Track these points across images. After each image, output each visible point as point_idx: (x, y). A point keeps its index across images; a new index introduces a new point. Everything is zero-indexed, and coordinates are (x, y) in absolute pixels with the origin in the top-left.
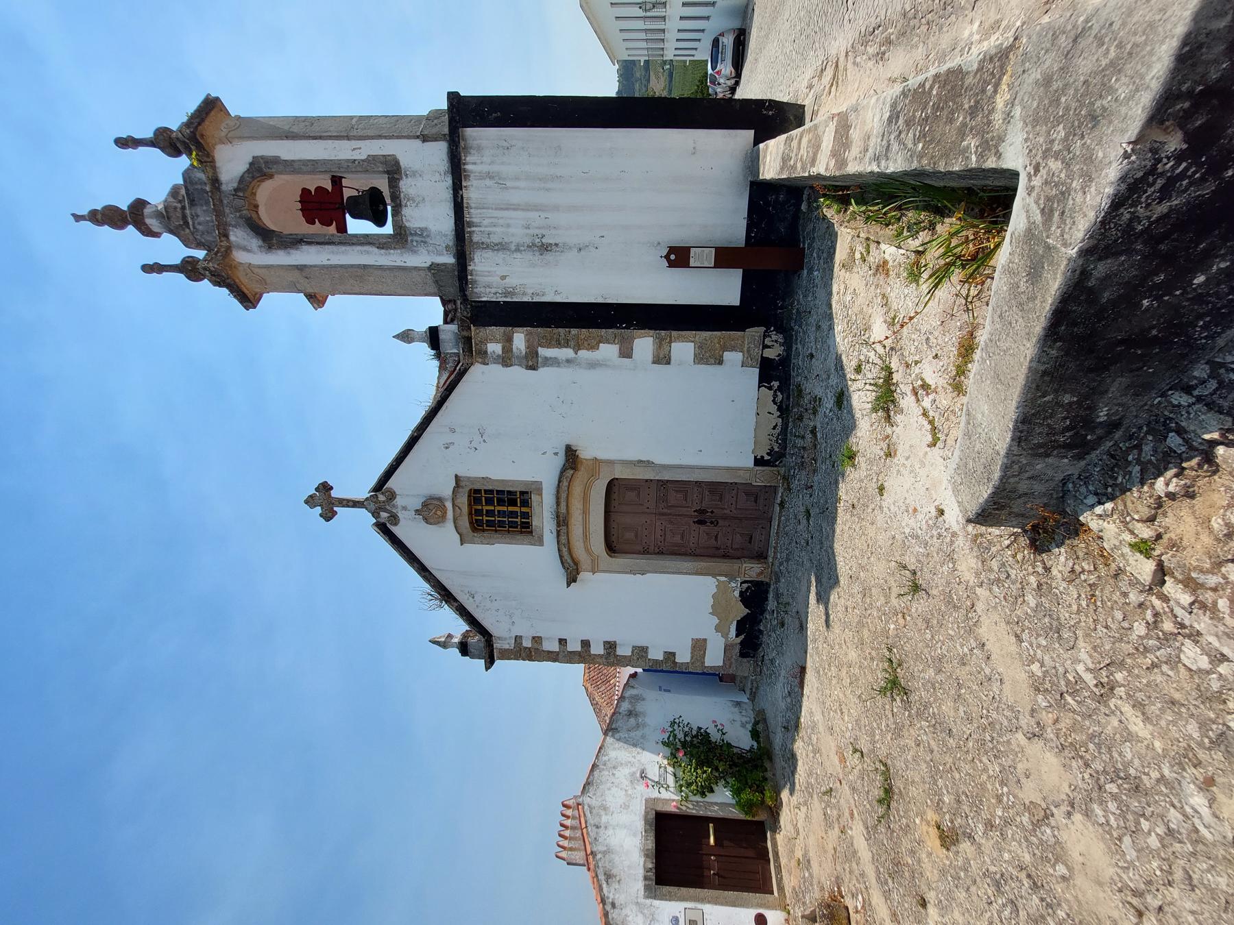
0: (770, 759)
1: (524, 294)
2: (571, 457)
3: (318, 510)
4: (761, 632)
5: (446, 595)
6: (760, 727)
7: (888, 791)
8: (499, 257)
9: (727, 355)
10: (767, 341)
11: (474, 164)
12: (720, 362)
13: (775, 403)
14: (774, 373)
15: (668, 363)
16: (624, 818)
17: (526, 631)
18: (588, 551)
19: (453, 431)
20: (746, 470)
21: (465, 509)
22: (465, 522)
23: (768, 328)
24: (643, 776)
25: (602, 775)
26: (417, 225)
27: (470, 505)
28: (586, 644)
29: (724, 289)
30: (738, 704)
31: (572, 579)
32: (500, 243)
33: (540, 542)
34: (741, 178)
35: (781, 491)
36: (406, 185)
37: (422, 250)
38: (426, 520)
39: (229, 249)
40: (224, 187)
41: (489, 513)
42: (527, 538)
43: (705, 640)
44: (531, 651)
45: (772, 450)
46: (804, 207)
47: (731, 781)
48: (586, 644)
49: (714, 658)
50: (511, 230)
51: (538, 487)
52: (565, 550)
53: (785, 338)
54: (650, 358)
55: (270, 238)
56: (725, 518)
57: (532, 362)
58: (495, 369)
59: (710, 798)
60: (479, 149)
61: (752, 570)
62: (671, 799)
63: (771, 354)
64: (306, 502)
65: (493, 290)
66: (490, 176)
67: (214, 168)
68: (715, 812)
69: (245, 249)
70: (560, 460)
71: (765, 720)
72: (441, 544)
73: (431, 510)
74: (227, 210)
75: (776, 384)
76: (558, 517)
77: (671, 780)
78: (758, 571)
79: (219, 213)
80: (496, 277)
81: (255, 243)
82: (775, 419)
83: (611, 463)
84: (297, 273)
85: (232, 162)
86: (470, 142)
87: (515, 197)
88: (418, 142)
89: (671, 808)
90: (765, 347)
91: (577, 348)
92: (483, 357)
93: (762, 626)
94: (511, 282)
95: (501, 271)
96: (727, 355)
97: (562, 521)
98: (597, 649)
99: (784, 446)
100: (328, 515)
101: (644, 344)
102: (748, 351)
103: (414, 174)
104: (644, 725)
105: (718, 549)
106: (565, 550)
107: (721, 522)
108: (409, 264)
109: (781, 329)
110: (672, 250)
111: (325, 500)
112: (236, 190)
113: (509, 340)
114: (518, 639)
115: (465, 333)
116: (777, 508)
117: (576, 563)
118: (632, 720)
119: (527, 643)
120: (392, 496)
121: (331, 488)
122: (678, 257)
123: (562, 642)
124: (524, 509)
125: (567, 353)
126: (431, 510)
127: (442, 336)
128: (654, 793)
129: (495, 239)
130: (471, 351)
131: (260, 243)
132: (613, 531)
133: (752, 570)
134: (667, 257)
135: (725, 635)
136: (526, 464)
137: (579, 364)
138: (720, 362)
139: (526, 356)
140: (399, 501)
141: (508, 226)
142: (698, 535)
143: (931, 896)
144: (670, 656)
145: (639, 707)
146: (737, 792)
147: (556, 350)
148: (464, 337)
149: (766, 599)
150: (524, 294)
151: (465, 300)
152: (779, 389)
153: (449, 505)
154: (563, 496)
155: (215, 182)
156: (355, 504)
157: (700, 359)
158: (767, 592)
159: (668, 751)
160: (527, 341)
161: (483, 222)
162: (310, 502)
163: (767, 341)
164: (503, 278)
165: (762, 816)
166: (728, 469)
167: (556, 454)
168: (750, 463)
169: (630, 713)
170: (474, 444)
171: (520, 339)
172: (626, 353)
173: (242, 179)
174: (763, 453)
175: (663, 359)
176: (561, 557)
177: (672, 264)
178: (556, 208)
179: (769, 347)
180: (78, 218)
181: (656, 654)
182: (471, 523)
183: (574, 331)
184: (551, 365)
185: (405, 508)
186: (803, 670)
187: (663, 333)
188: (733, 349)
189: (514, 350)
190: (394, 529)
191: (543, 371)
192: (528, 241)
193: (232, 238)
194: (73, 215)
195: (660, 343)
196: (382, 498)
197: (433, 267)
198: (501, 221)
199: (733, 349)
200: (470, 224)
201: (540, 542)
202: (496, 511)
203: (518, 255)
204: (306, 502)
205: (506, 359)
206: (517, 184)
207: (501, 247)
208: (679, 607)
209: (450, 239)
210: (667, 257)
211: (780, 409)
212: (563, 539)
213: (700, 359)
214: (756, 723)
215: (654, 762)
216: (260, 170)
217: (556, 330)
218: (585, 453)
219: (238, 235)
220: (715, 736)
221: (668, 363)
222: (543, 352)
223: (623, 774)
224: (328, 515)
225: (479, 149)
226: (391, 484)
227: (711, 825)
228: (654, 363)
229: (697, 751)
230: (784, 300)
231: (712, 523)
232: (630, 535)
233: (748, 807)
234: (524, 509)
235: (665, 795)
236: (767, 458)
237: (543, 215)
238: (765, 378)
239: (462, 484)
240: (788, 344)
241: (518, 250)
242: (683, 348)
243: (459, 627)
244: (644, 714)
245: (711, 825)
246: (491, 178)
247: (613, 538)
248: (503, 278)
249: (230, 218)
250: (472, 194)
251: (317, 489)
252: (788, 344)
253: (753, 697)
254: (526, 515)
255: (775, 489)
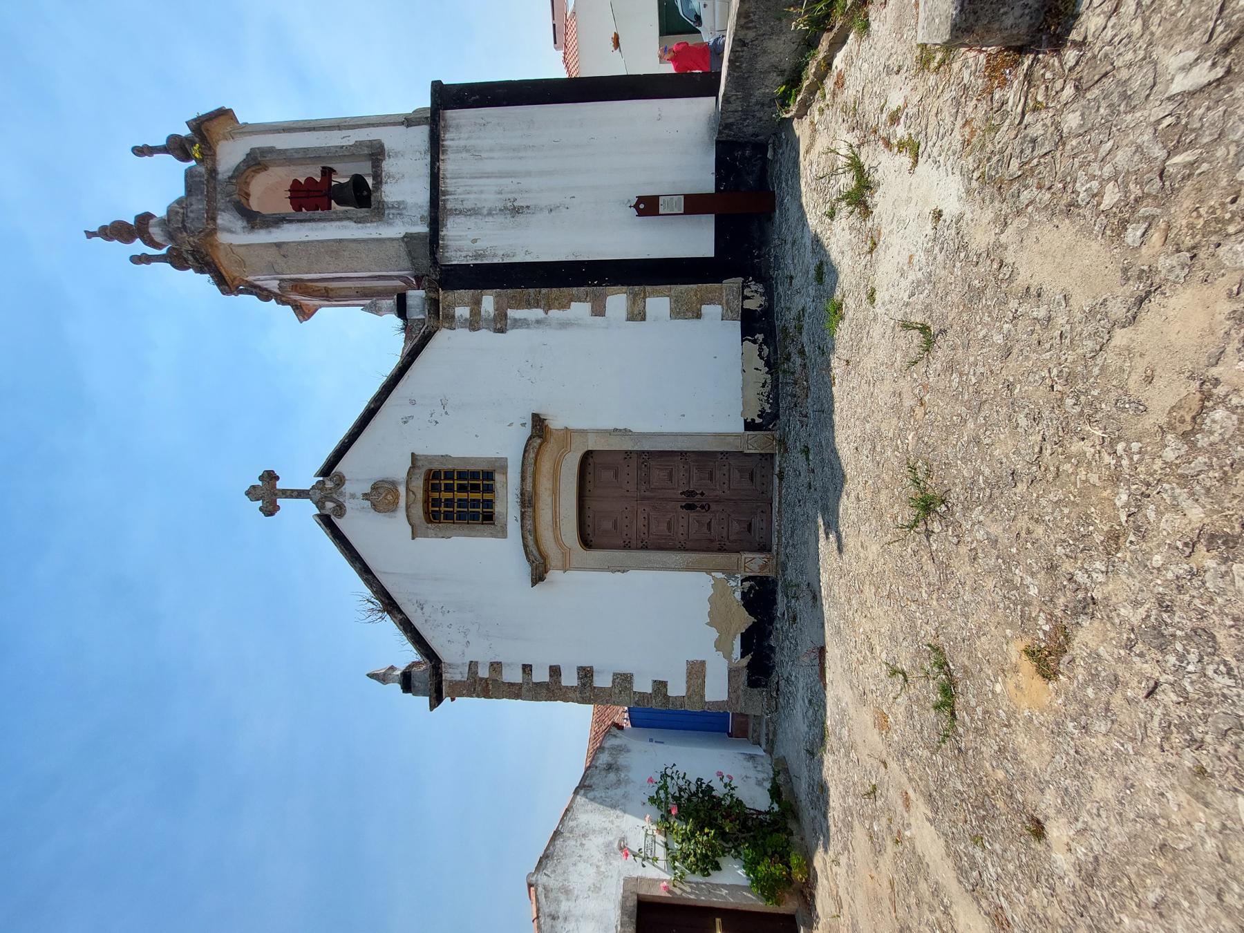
0: (796, 817)
1: (495, 255)
2: (539, 424)
3: (260, 503)
4: (772, 649)
5: (390, 605)
6: (781, 779)
7: (948, 691)
8: (471, 222)
9: (706, 309)
10: (747, 292)
11: (451, 140)
12: (698, 316)
13: (762, 358)
14: (754, 325)
15: (644, 319)
16: (591, 905)
17: (483, 655)
18: (557, 540)
19: (413, 403)
20: (737, 435)
21: (420, 495)
22: (418, 510)
23: (746, 279)
24: (624, 849)
25: (569, 845)
26: (394, 199)
27: (426, 491)
28: (555, 671)
29: (696, 239)
30: (752, 757)
31: (538, 577)
32: (473, 209)
33: (503, 533)
34: (706, 138)
35: (777, 459)
36: (388, 166)
37: (398, 221)
38: (375, 507)
39: (213, 232)
40: (220, 177)
41: (449, 503)
42: (487, 528)
43: (703, 663)
44: (487, 685)
45: (763, 411)
46: (770, 155)
47: (745, 848)
48: (555, 671)
49: (717, 690)
50: (483, 196)
51: (502, 465)
52: (530, 538)
53: (765, 288)
54: (624, 315)
55: (254, 220)
56: (718, 501)
57: (500, 324)
58: (462, 334)
59: (716, 878)
60: (458, 127)
61: (754, 563)
62: (659, 877)
63: (752, 305)
64: (248, 493)
65: (464, 254)
66: (466, 149)
67: (214, 161)
68: (723, 899)
69: (230, 231)
70: (527, 431)
71: (786, 771)
72: (388, 537)
73: (381, 496)
74: (219, 197)
75: (760, 337)
76: (522, 494)
77: (660, 852)
78: (761, 562)
79: (211, 199)
80: (466, 241)
81: (240, 224)
82: (763, 375)
83: (583, 432)
84: (274, 250)
85: (230, 155)
86: (450, 122)
87: (488, 166)
88: (403, 128)
89: (660, 892)
90: (745, 298)
91: (548, 307)
92: (450, 321)
93: (771, 629)
94: (480, 245)
95: (472, 235)
96: (706, 309)
97: (528, 502)
98: (570, 679)
99: (776, 404)
100: (270, 510)
101: (617, 301)
102: (727, 303)
103: (396, 154)
104: (627, 782)
105: (711, 541)
106: (530, 538)
107: (714, 507)
108: (384, 236)
109: (758, 279)
110: (641, 199)
111: (268, 493)
112: (230, 178)
113: (478, 302)
114: (473, 665)
115: (432, 295)
116: (776, 481)
117: (544, 558)
118: (612, 776)
119: (484, 673)
120: (341, 481)
121: (277, 478)
122: (648, 206)
123: (527, 669)
124: (487, 496)
125: (538, 313)
126: (381, 496)
127: (410, 302)
128: (635, 869)
129: (468, 205)
130: (438, 315)
131: (245, 224)
132: (589, 521)
133: (754, 563)
134: (636, 206)
135: (728, 656)
136: (492, 440)
137: (549, 325)
138: (698, 316)
139: (495, 319)
140: (348, 488)
141: (482, 192)
142: (687, 523)
143: (1047, 804)
144: (660, 686)
145: (622, 760)
146: (751, 866)
147: (526, 311)
148: (431, 299)
149: (774, 602)
150: (495, 255)
151: (435, 262)
152: (765, 342)
153: (402, 490)
154: (530, 470)
155: (213, 172)
156: (301, 494)
157: (679, 312)
158: (774, 592)
159: (656, 813)
160: (496, 303)
161: (457, 190)
162: (252, 493)
163: (747, 292)
164: (474, 241)
165: (789, 906)
166: (717, 435)
167: (523, 425)
168: (740, 428)
169: (609, 767)
170: (434, 418)
171: (488, 302)
172: (599, 311)
173: (237, 168)
174: (753, 415)
175: (636, 315)
176: (525, 546)
177: (641, 213)
178: (528, 174)
179: (749, 298)
180: (90, 235)
181: (643, 685)
182: (426, 513)
183: (544, 291)
184: (520, 327)
185: (353, 496)
186: (822, 651)
187: (637, 288)
188: (711, 302)
189: (483, 313)
190: (340, 523)
191: (512, 335)
192: (500, 205)
193: (219, 221)
194: (86, 232)
195: (634, 299)
196: (329, 484)
197: (409, 239)
198: (475, 189)
199: (711, 302)
200: (445, 193)
201: (503, 533)
202: (454, 497)
203: (491, 219)
204: (248, 493)
205: (474, 324)
206: (491, 155)
207: (474, 212)
208: (667, 619)
209: (425, 210)
210: (636, 206)
211: (767, 364)
212: (529, 523)
213: (679, 312)
214: (777, 774)
215: (639, 828)
216: (256, 162)
217: (526, 291)
218: (556, 423)
219: (224, 219)
220: (719, 790)
221: (644, 319)
222: (511, 313)
223: (595, 844)
224: (270, 510)
225: (458, 127)
226: (341, 467)
227: (718, 920)
228: (628, 320)
229: (702, 817)
230: (760, 249)
231: (703, 507)
232: (607, 525)
233: (769, 887)
234: (487, 496)
235: (651, 872)
236: (758, 421)
237: (515, 181)
238: (747, 332)
239: (420, 464)
240: (769, 293)
241: (490, 214)
242: (658, 304)
243: (405, 655)
244: (627, 768)
245: (718, 920)
246: (468, 151)
247: (589, 530)
248: (474, 241)
249: (221, 202)
250: (449, 166)
251: (261, 478)
252: (769, 293)
253: (770, 751)
254: (489, 504)
255: (772, 455)
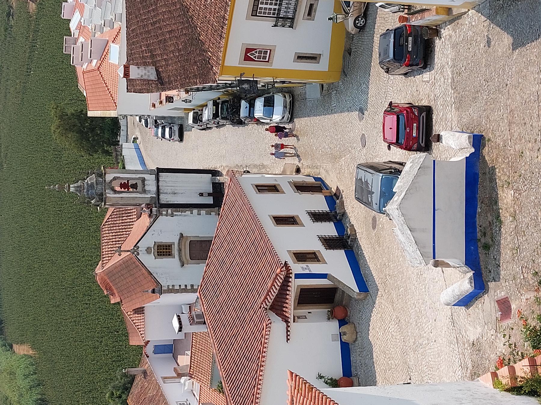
2: (182, 235)
12: (211, 214)
17: (170, 284)
18: (186, 258)
22: (156, 253)
29: (210, 200)
55: (115, 192)
73: (148, 250)
81: (112, 192)
97: (180, 250)
98: (189, 287)
101: (195, 211)
114: (168, 286)
119: (171, 287)
122: (201, 195)
123: (180, 286)
126: (148, 250)
130: (160, 214)
136: (172, 238)
138: (211, 214)
153: (153, 249)
155: (105, 181)
157: (206, 214)
171: (170, 211)
205: (167, 215)
213: (206, 214)
216: (115, 179)
242: (203, 212)
249: (107, 188)
250: (160, 184)
